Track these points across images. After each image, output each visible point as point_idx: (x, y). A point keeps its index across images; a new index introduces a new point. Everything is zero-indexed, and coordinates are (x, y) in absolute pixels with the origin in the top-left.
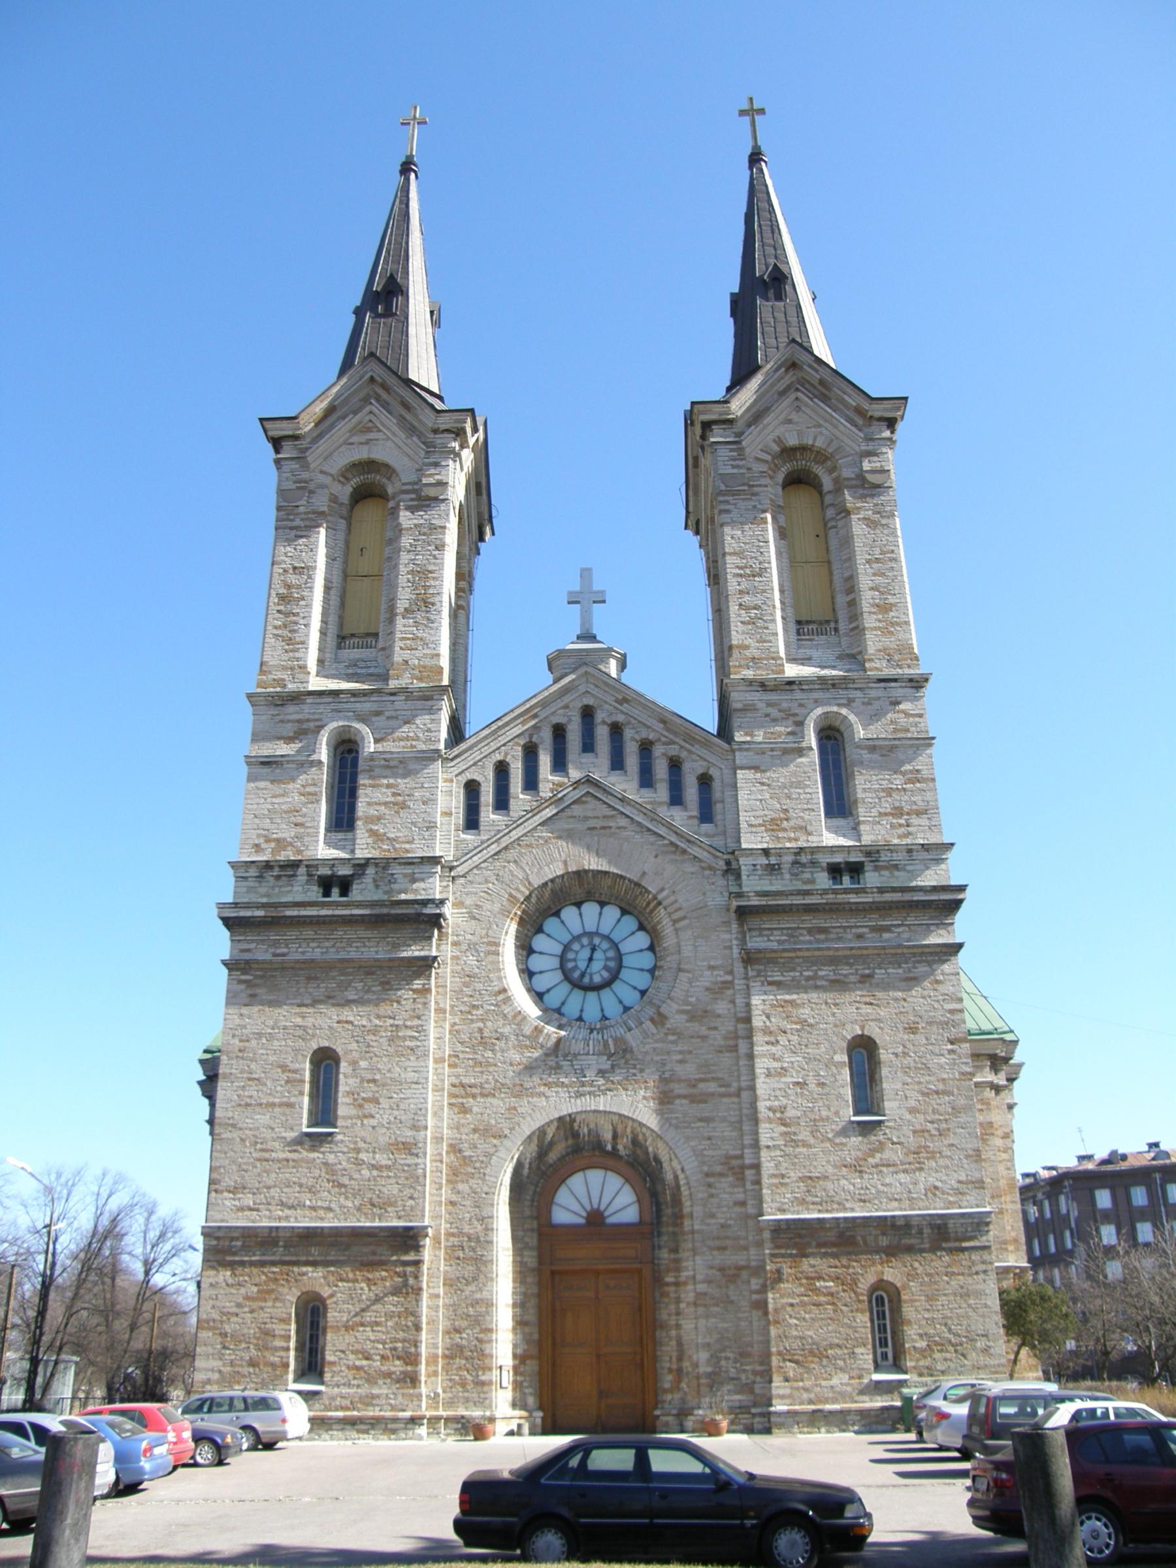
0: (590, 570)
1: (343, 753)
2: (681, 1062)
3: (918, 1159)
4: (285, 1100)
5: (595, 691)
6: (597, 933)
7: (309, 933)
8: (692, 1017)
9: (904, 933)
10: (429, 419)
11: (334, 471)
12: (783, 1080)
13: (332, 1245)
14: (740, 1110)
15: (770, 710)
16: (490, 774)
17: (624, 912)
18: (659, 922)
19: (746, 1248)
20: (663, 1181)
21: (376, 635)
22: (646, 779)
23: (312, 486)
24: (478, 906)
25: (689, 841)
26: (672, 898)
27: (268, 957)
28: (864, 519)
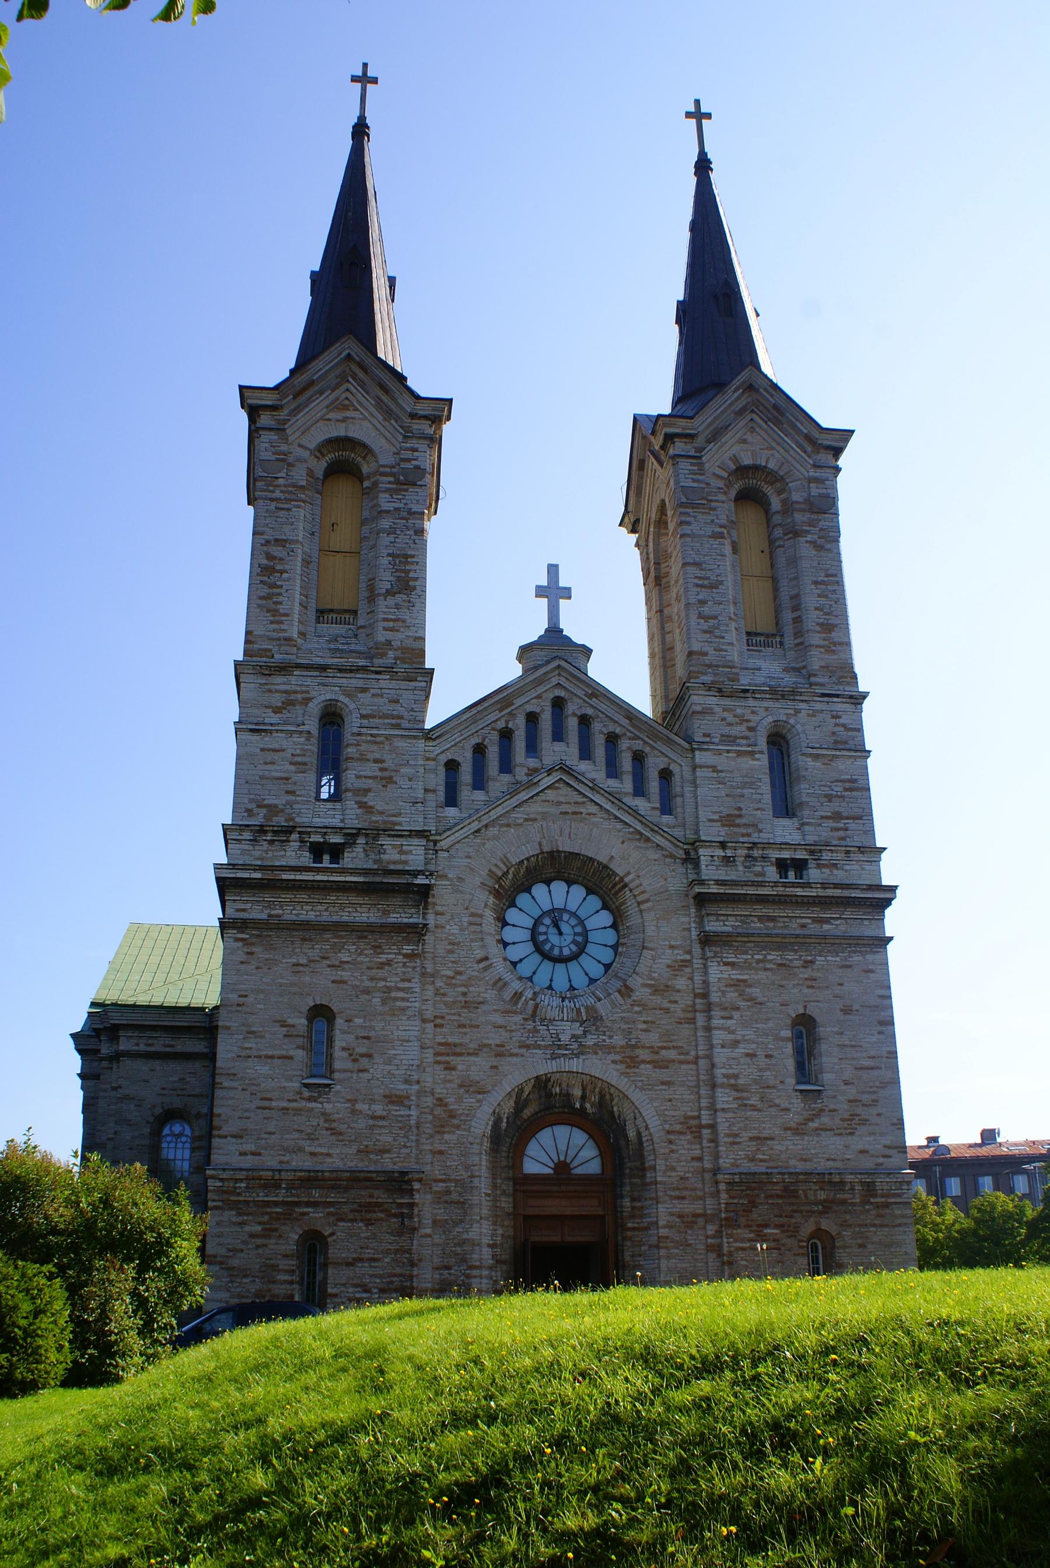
0: (557, 566)
1: (324, 725)
2: (645, 1031)
3: (852, 1124)
4: (284, 1053)
5: (567, 685)
6: (565, 910)
7: (303, 896)
8: (656, 990)
9: (838, 925)
10: (408, 405)
11: (312, 446)
12: (736, 1050)
13: (332, 1187)
14: (698, 1076)
15: (726, 714)
16: (469, 754)
17: (590, 891)
18: (623, 903)
19: (702, 1198)
20: (626, 1137)
21: (355, 612)
22: (613, 770)
23: (291, 459)
24: (461, 879)
25: (653, 830)
26: (637, 882)
27: (264, 916)
28: (810, 542)
